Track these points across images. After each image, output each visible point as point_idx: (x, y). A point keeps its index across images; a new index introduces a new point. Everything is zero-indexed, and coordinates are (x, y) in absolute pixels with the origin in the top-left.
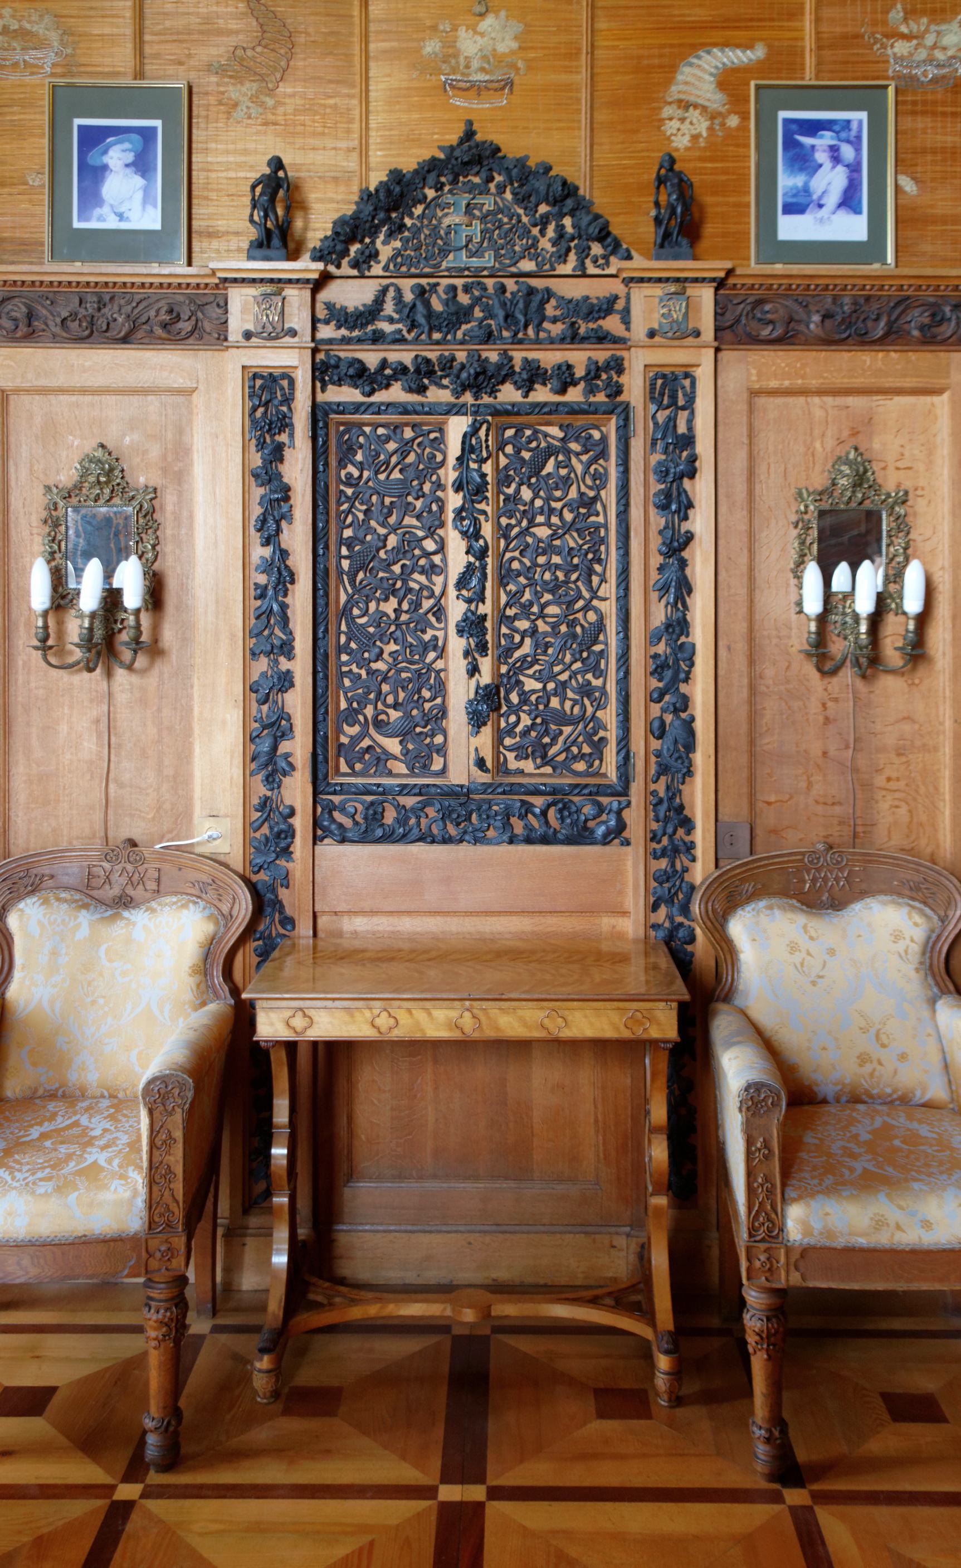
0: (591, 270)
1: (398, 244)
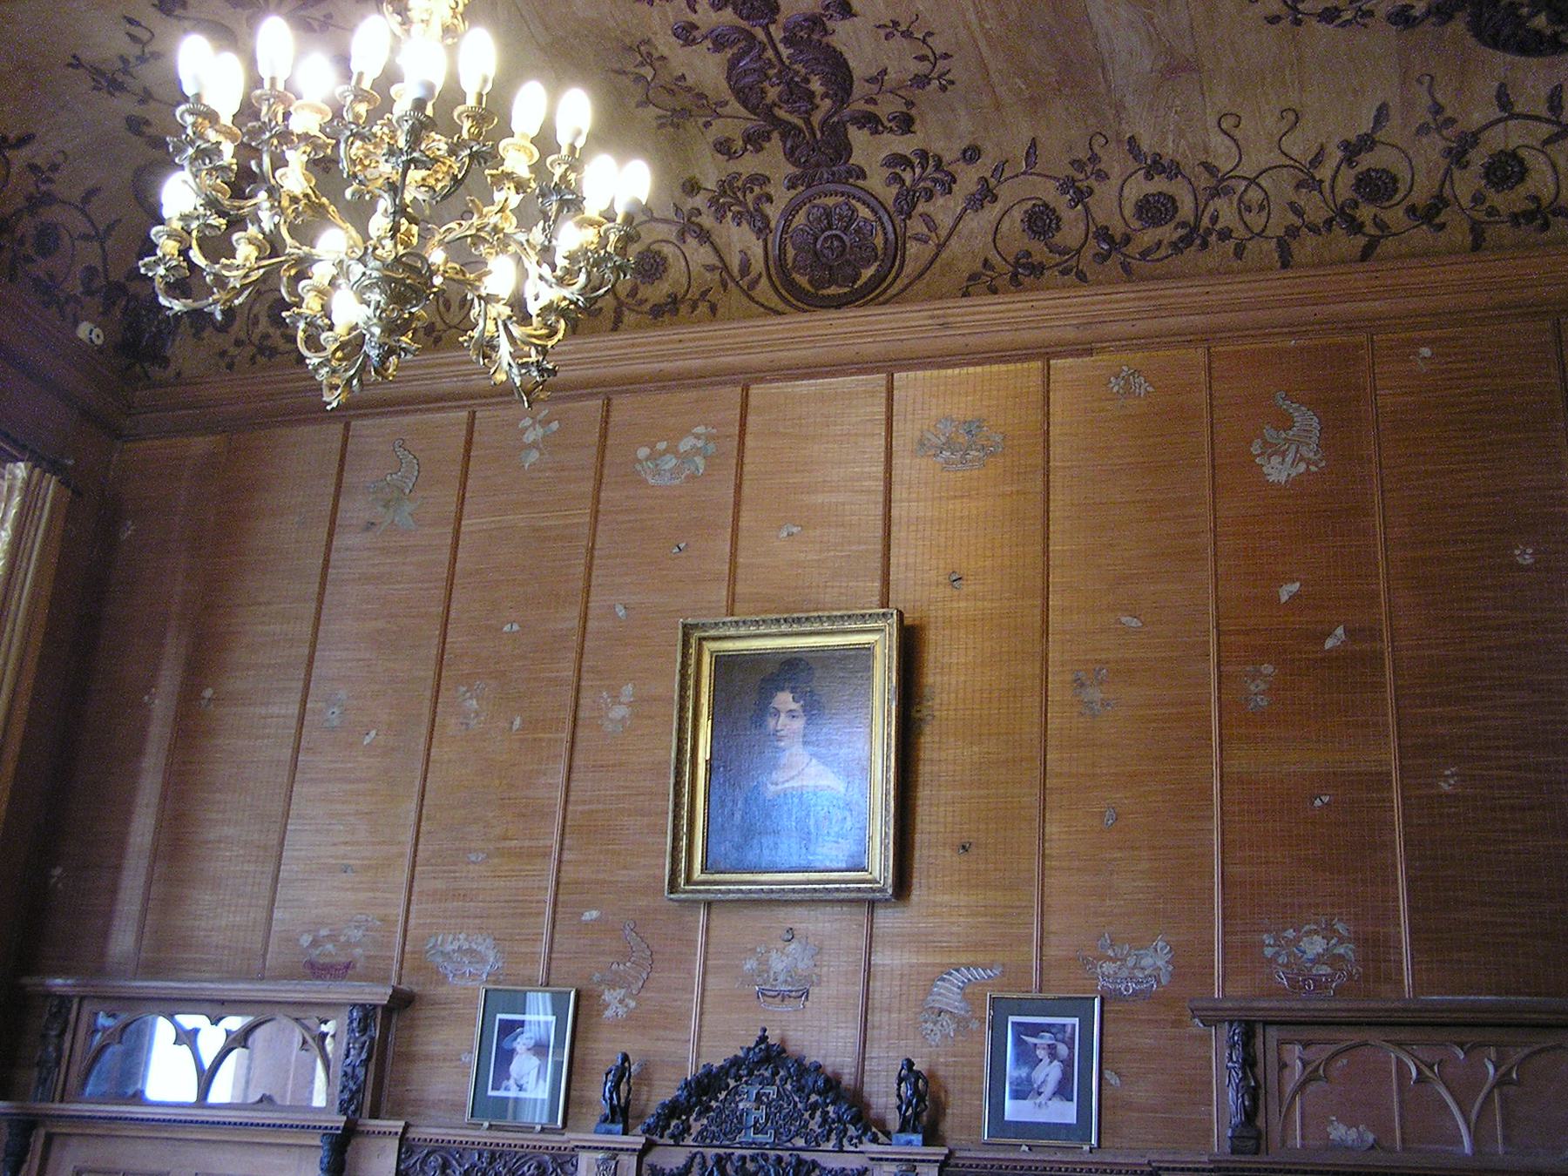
0: (847, 1147)
1: (705, 1121)
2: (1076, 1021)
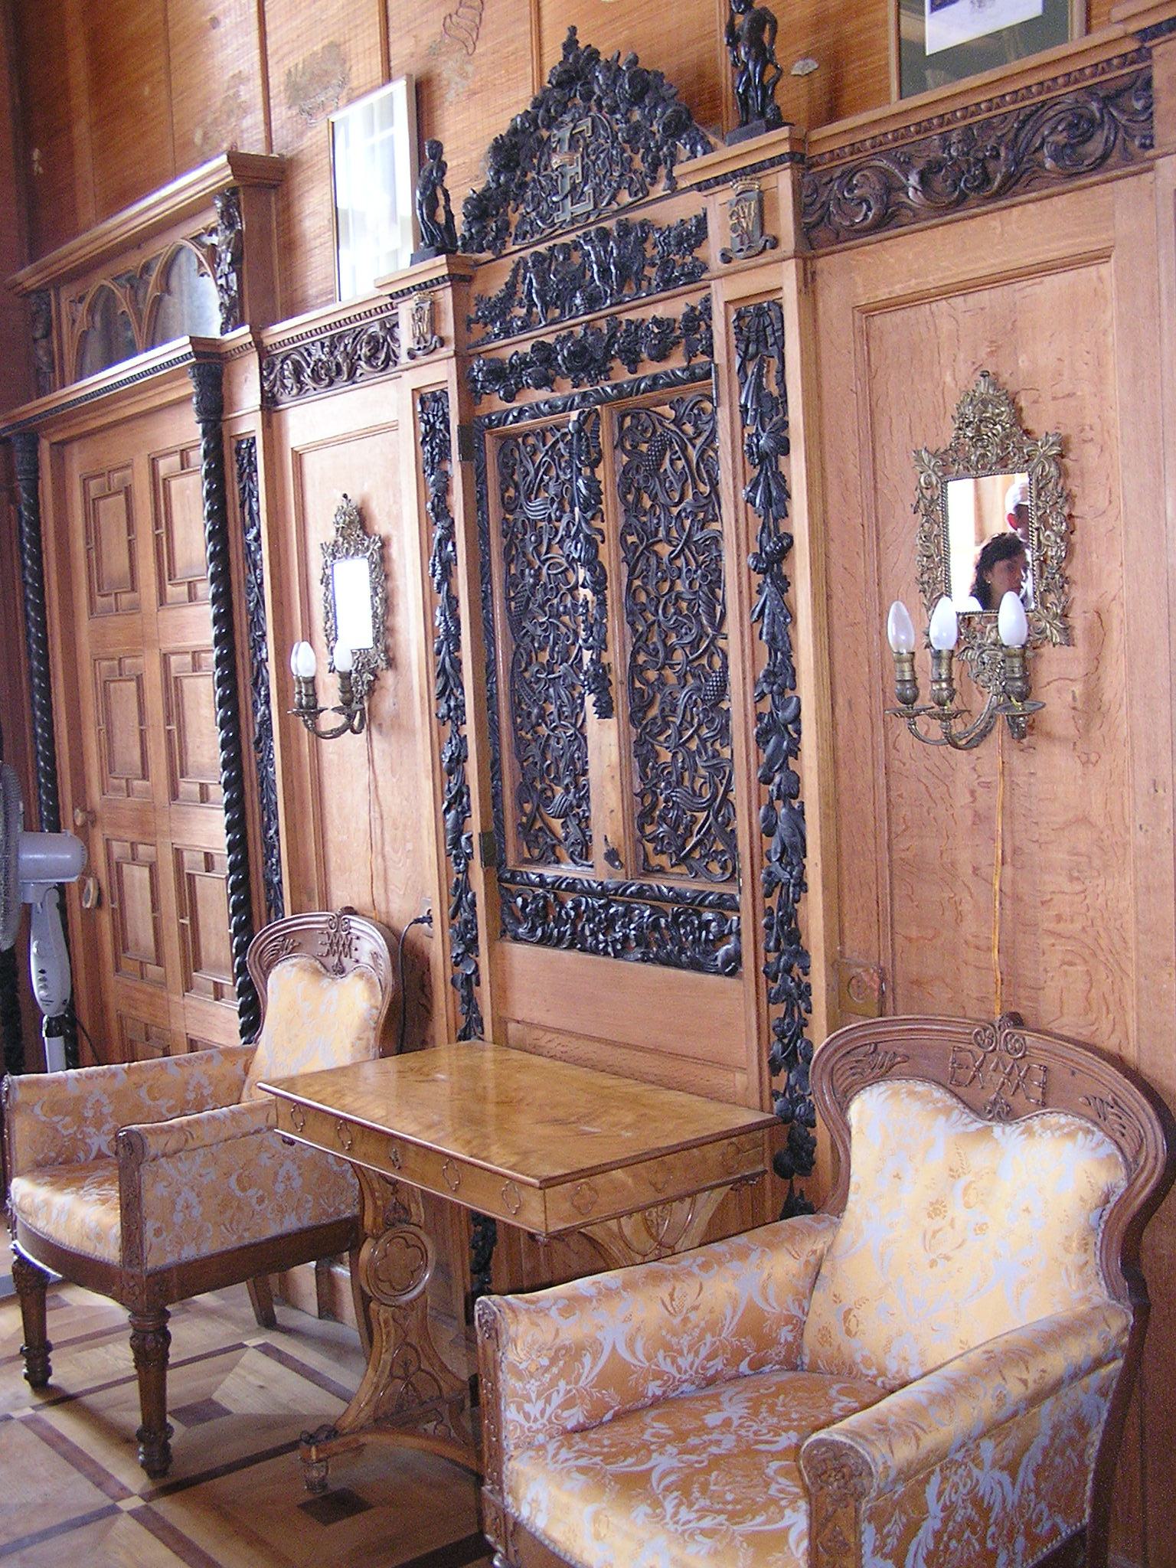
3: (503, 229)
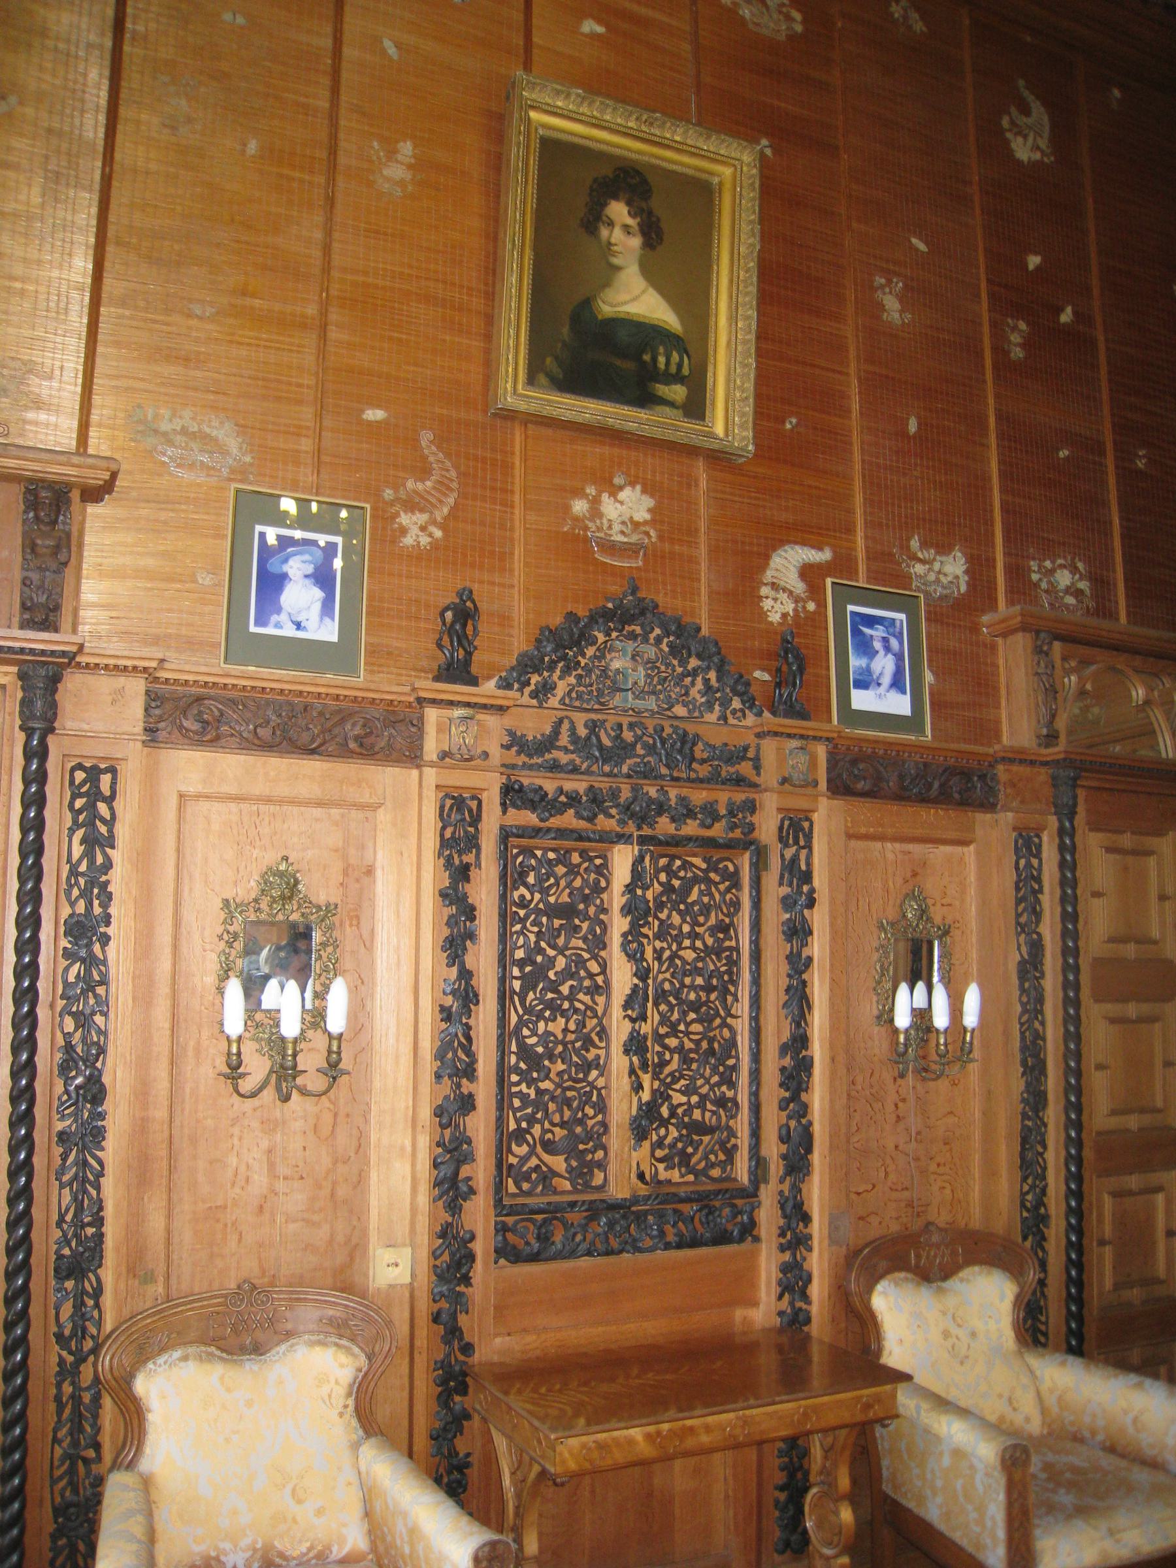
0: (731, 721)
2: (903, 616)
3: (546, 689)
